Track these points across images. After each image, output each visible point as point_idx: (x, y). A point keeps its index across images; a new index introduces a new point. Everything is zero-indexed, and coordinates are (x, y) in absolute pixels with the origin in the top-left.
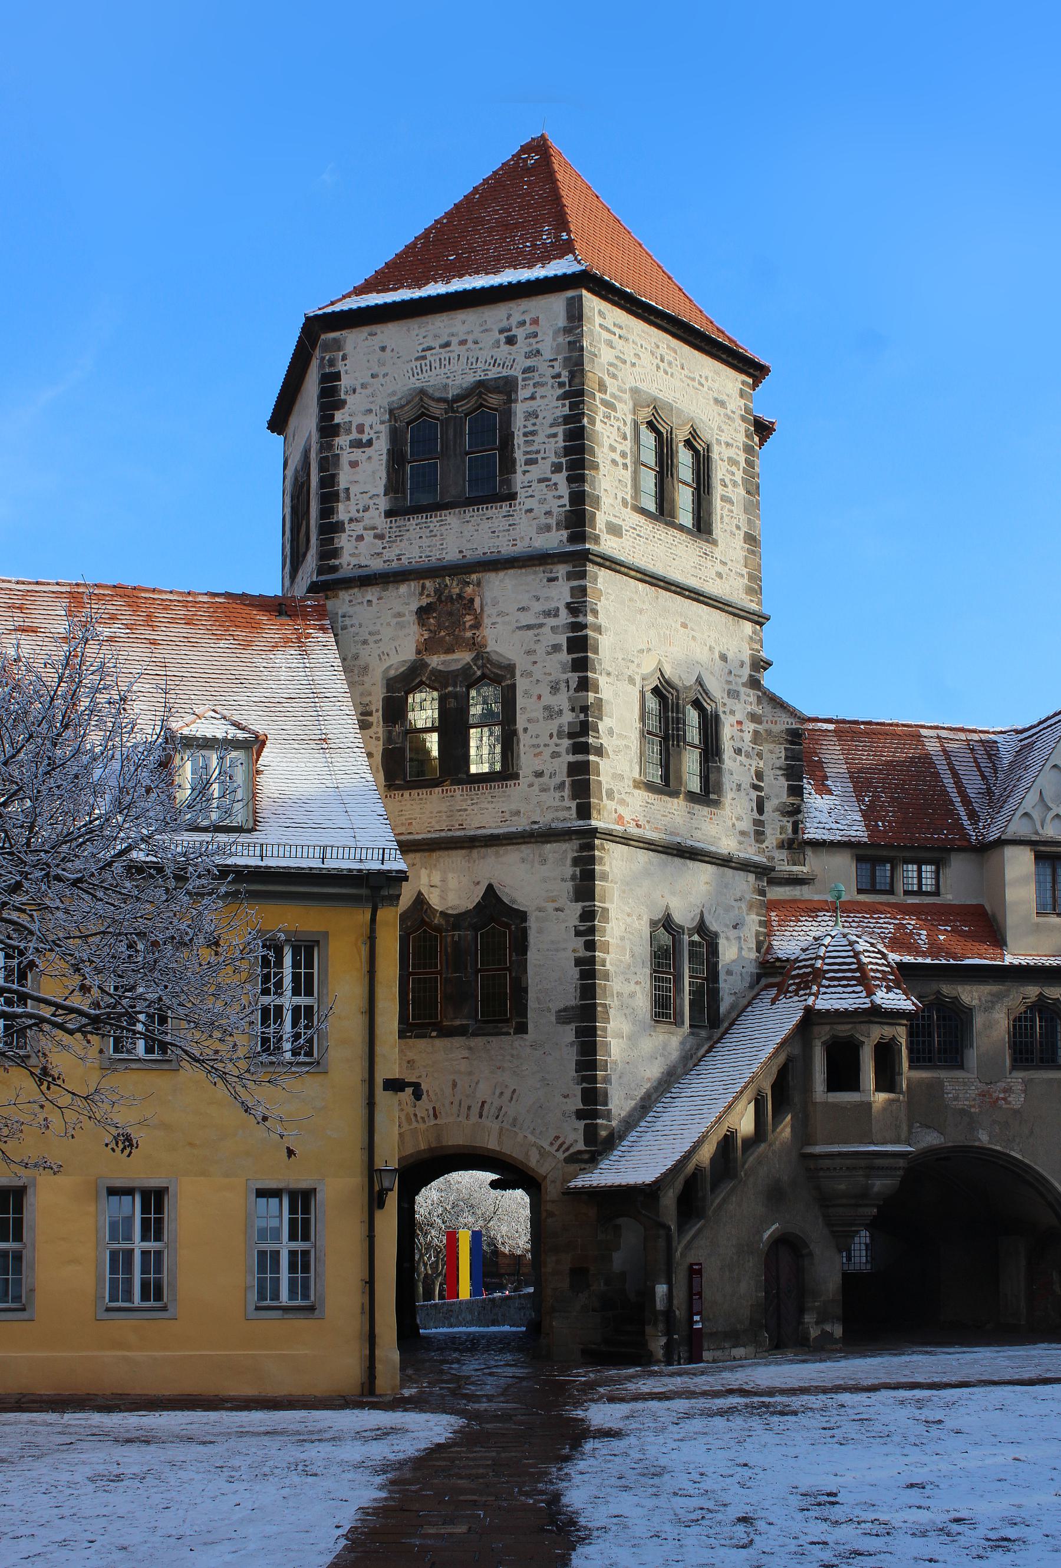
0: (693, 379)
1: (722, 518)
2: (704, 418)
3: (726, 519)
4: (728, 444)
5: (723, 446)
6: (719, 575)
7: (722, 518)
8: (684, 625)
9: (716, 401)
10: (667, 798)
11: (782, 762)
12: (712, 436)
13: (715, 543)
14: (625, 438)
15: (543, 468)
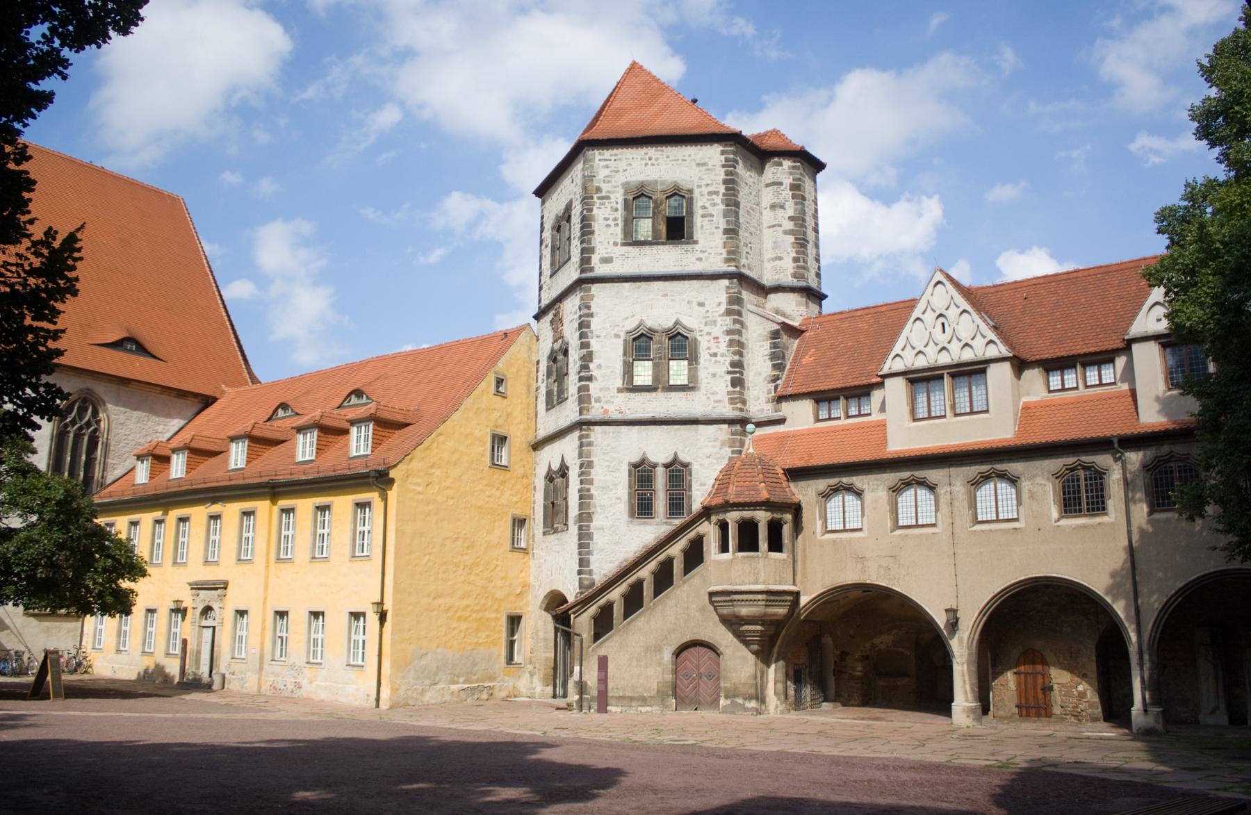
0: (678, 160)
1: (702, 227)
2: (687, 178)
3: (705, 228)
4: (708, 185)
5: (704, 187)
6: (700, 259)
7: (702, 227)
8: (665, 295)
9: (698, 165)
10: (647, 393)
11: (768, 351)
12: (693, 185)
13: (696, 242)
14: (617, 210)
15: (577, 239)
